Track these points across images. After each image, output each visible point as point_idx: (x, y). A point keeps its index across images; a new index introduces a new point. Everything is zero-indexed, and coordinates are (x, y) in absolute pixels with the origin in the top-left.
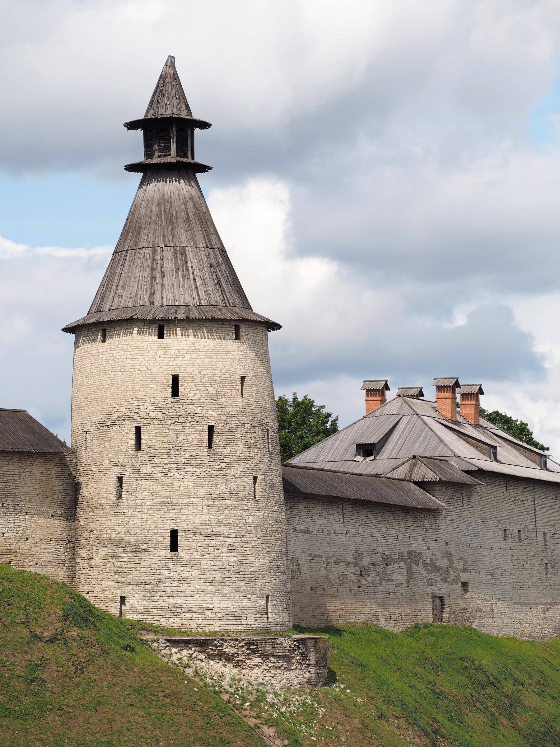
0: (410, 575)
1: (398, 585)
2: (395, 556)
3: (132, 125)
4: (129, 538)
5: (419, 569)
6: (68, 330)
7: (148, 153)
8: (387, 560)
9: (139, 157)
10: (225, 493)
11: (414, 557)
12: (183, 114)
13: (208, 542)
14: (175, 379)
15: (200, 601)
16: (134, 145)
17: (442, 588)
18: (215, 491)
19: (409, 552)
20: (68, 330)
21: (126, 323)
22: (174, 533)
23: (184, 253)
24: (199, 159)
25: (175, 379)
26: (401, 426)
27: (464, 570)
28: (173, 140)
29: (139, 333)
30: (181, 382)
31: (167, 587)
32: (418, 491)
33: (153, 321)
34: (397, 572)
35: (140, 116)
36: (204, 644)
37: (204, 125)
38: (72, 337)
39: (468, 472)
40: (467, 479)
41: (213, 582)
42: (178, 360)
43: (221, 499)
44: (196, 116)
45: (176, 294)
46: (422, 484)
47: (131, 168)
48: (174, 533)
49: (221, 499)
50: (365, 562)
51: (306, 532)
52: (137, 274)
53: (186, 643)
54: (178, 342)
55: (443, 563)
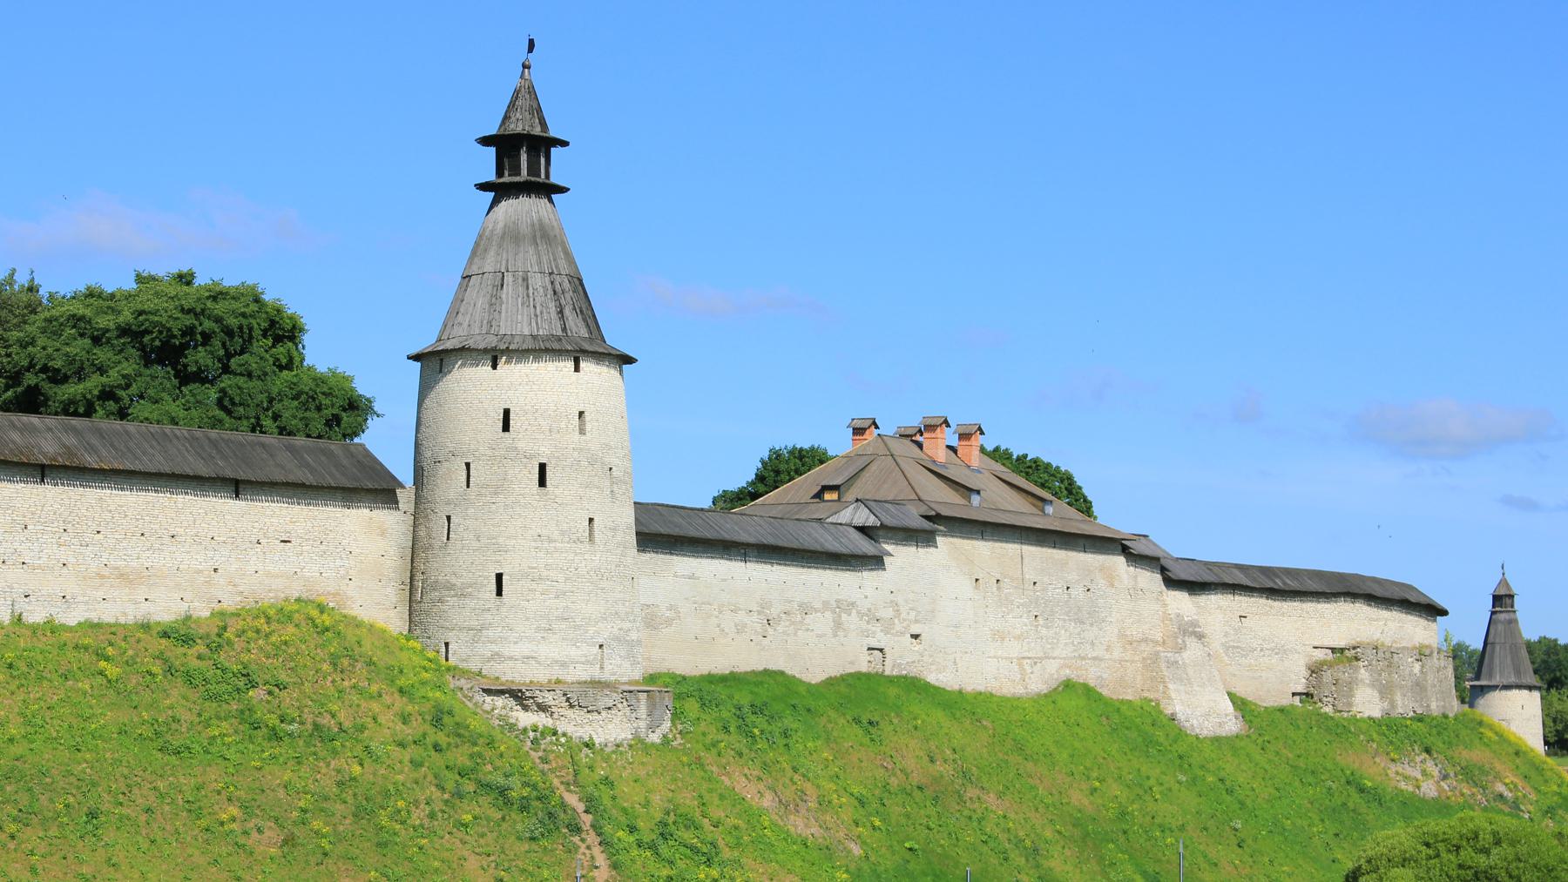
0: (838, 625)
1: (819, 636)
2: (818, 605)
3: (485, 141)
4: (454, 580)
5: (851, 621)
6: (416, 358)
7: (500, 173)
8: (806, 610)
9: (491, 176)
10: (556, 535)
12: (537, 131)
13: (534, 586)
14: (507, 413)
15: (524, 648)
16: (485, 164)
18: (544, 532)
19: (837, 601)
20: (416, 358)
21: (465, 353)
22: (499, 577)
23: (525, 279)
24: (555, 179)
25: (507, 413)
26: (873, 467)
27: (917, 621)
28: (524, 157)
29: (507, 362)
30: (512, 416)
31: (490, 633)
32: (856, 535)
33: (485, 351)
34: (821, 623)
35: (494, 132)
36: (518, 696)
37: (564, 144)
38: (419, 364)
39: (927, 518)
40: (927, 525)
41: (538, 629)
42: (510, 393)
43: (550, 540)
44: (553, 132)
45: (517, 322)
46: (863, 530)
47: (484, 187)
48: (499, 577)
49: (550, 540)
50: (774, 612)
51: (692, 577)
52: (477, 298)
53: (500, 692)
54: (510, 371)
55: (887, 613)
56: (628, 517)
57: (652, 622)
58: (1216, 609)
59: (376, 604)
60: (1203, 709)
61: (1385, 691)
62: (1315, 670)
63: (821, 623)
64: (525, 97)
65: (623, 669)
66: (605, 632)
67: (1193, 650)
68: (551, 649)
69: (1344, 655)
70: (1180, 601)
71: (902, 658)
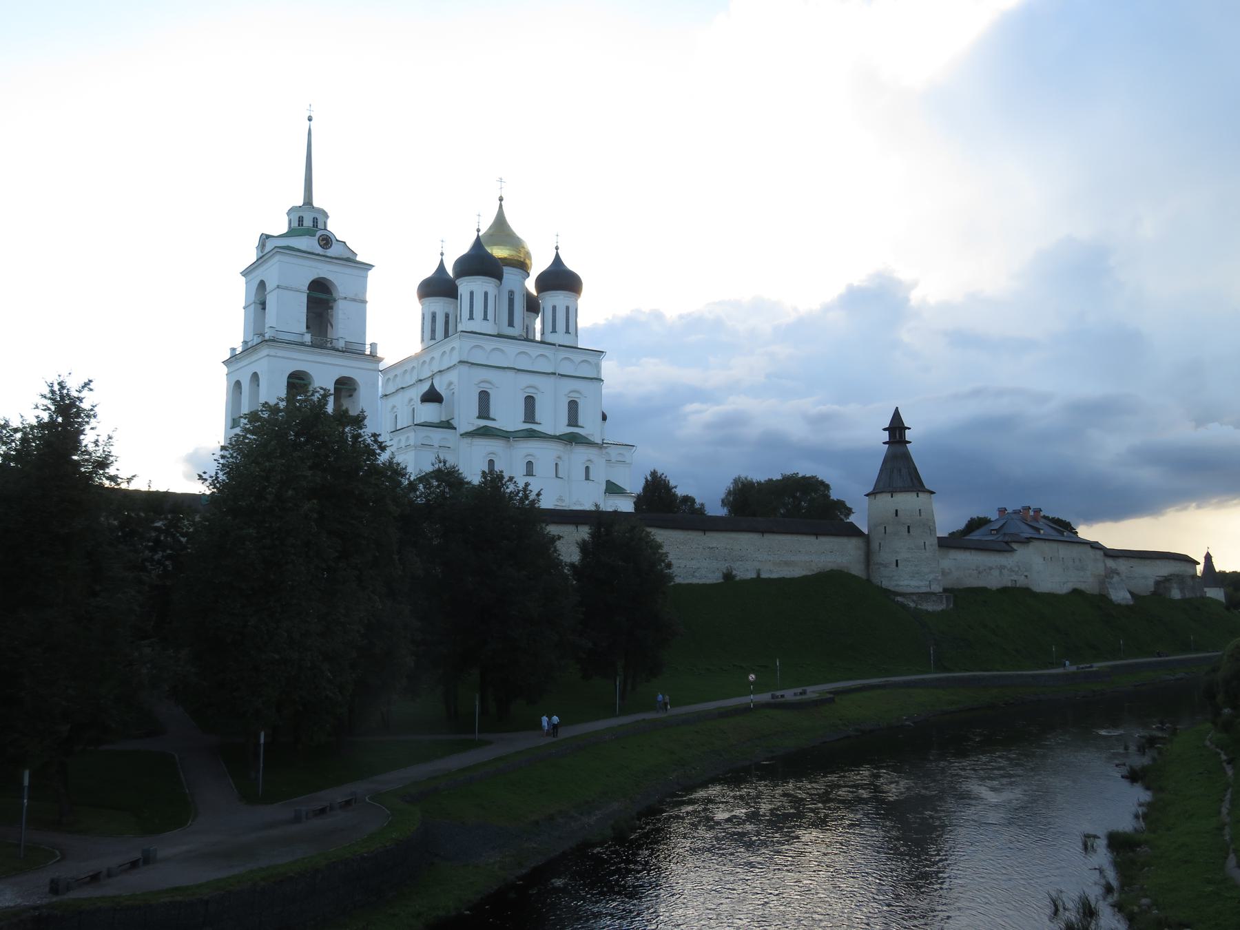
5: (1005, 572)
8: (991, 568)
11: (1002, 568)
15: (906, 583)
16: (886, 436)
17: (1014, 577)
56: (936, 541)
57: (944, 573)
58: (1122, 565)
59: (857, 570)
60: (1120, 595)
61: (1182, 590)
62: (1157, 583)
63: (996, 573)
64: (897, 415)
65: (936, 588)
66: (931, 577)
67: (1116, 579)
68: (913, 583)
69: (1167, 579)
70: (1111, 563)
71: (1021, 581)
